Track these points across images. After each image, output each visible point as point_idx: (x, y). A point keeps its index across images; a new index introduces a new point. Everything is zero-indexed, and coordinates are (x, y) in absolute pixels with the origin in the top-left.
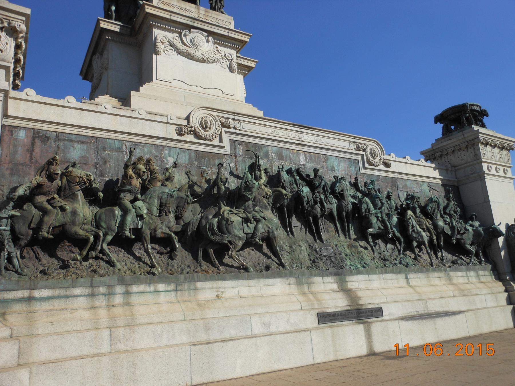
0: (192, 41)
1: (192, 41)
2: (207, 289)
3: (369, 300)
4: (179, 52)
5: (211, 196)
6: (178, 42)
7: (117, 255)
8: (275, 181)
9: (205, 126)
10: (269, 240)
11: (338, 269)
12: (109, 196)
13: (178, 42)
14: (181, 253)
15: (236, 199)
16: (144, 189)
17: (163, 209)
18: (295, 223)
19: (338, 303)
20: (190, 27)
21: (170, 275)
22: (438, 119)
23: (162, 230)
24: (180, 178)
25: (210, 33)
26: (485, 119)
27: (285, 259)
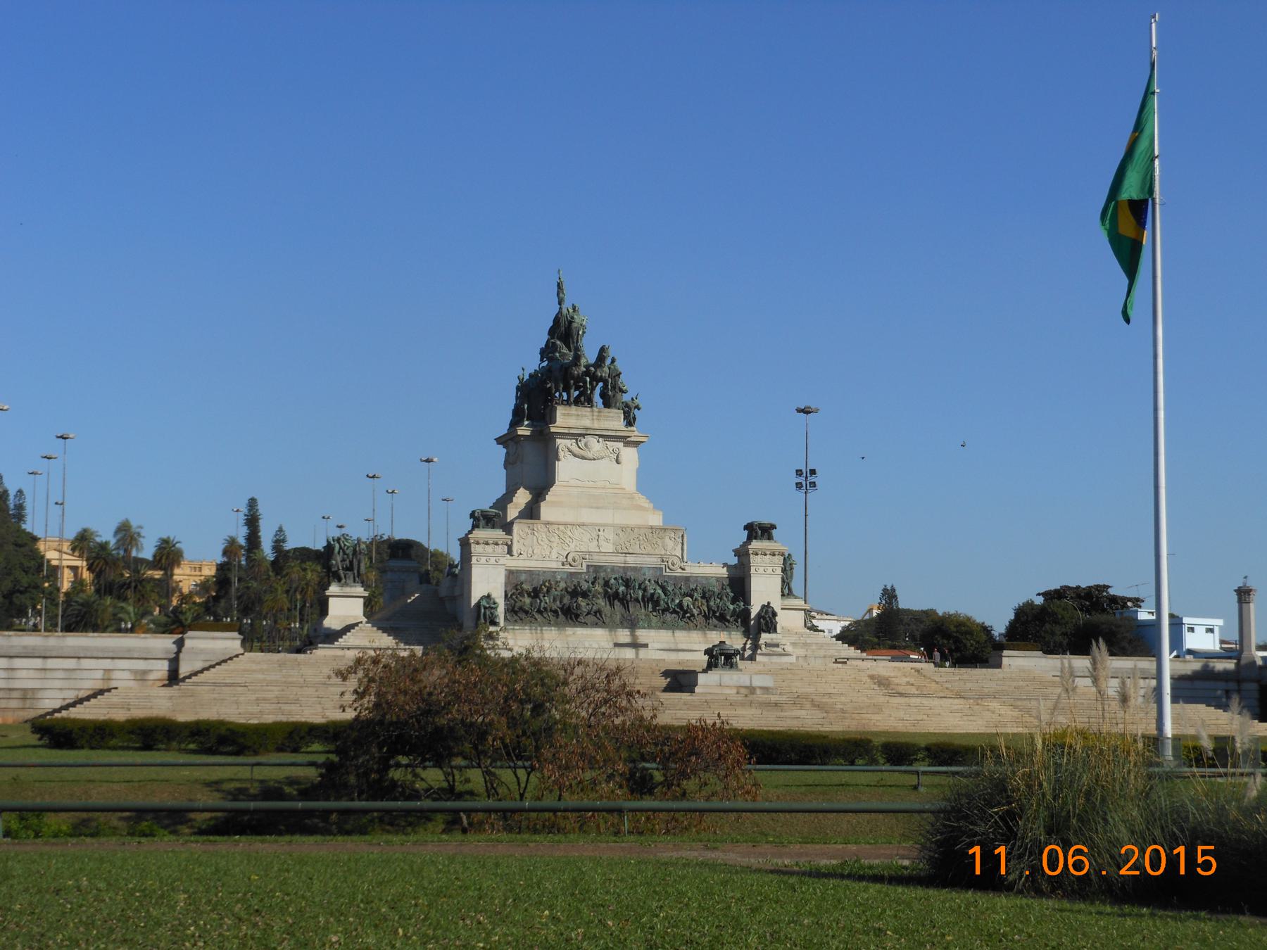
0: (586, 445)
1: (586, 445)
2: (569, 631)
3: (642, 640)
4: (575, 456)
5: (576, 593)
6: (574, 448)
7: (537, 616)
8: (607, 584)
9: (574, 560)
10: (599, 611)
11: (632, 625)
12: (535, 593)
13: (574, 448)
14: (561, 616)
15: (585, 595)
16: (548, 591)
17: (554, 600)
18: (616, 602)
19: (627, 640)
20: (583, 435)
21: (557, 625)
22: (746, 528)
23: (554, 607)
24: (562, 585)
25: (600, 436)
26: (774, 532)
27: (607, 620)
